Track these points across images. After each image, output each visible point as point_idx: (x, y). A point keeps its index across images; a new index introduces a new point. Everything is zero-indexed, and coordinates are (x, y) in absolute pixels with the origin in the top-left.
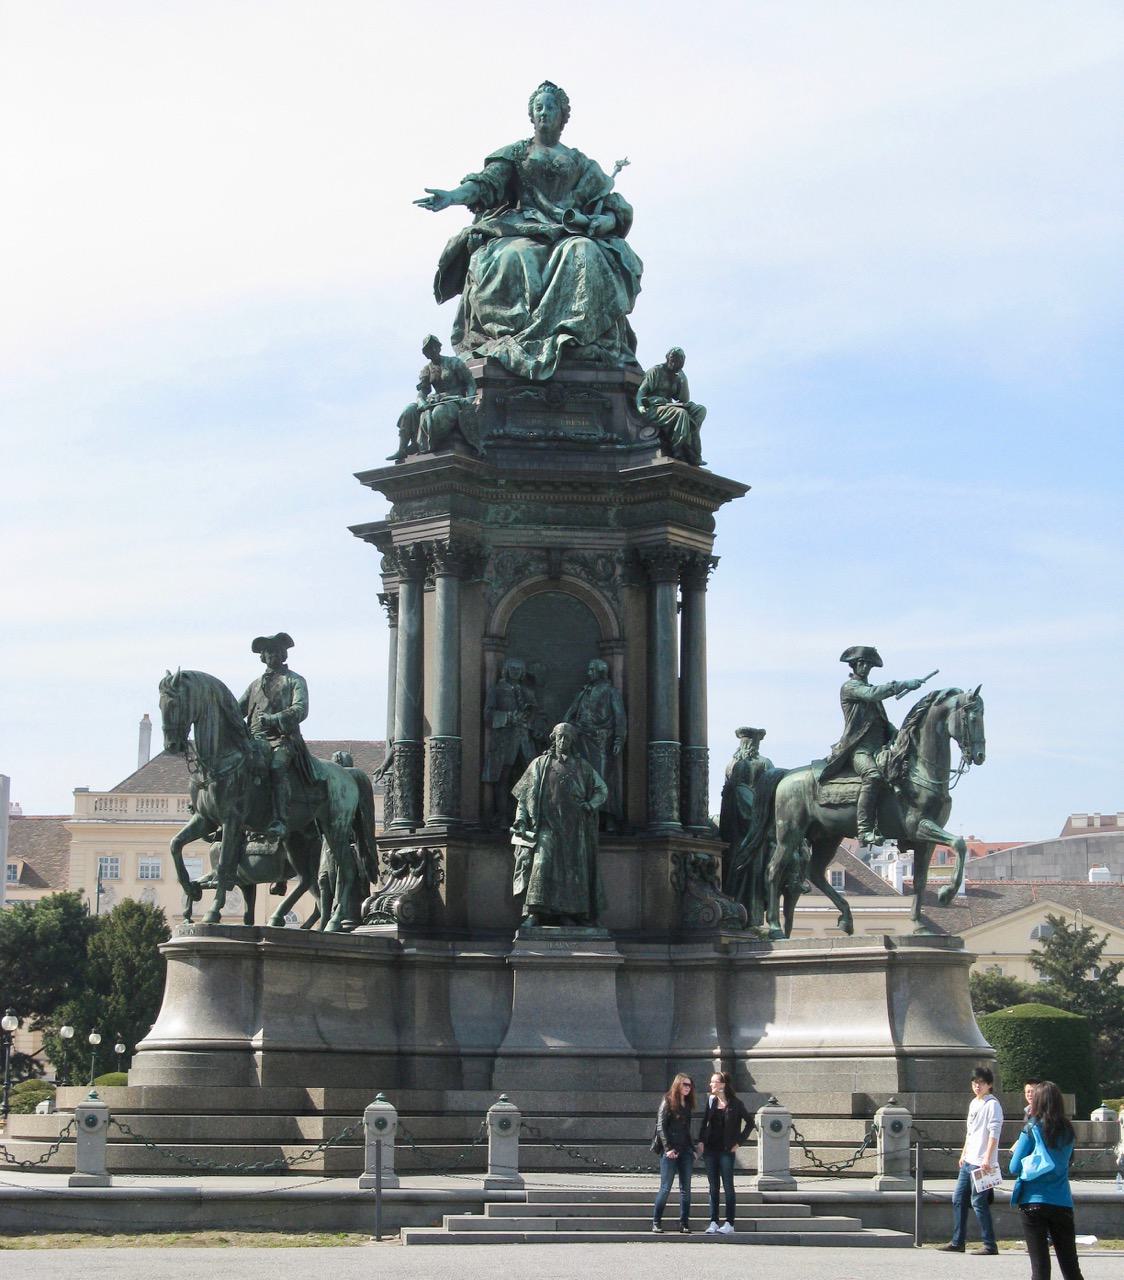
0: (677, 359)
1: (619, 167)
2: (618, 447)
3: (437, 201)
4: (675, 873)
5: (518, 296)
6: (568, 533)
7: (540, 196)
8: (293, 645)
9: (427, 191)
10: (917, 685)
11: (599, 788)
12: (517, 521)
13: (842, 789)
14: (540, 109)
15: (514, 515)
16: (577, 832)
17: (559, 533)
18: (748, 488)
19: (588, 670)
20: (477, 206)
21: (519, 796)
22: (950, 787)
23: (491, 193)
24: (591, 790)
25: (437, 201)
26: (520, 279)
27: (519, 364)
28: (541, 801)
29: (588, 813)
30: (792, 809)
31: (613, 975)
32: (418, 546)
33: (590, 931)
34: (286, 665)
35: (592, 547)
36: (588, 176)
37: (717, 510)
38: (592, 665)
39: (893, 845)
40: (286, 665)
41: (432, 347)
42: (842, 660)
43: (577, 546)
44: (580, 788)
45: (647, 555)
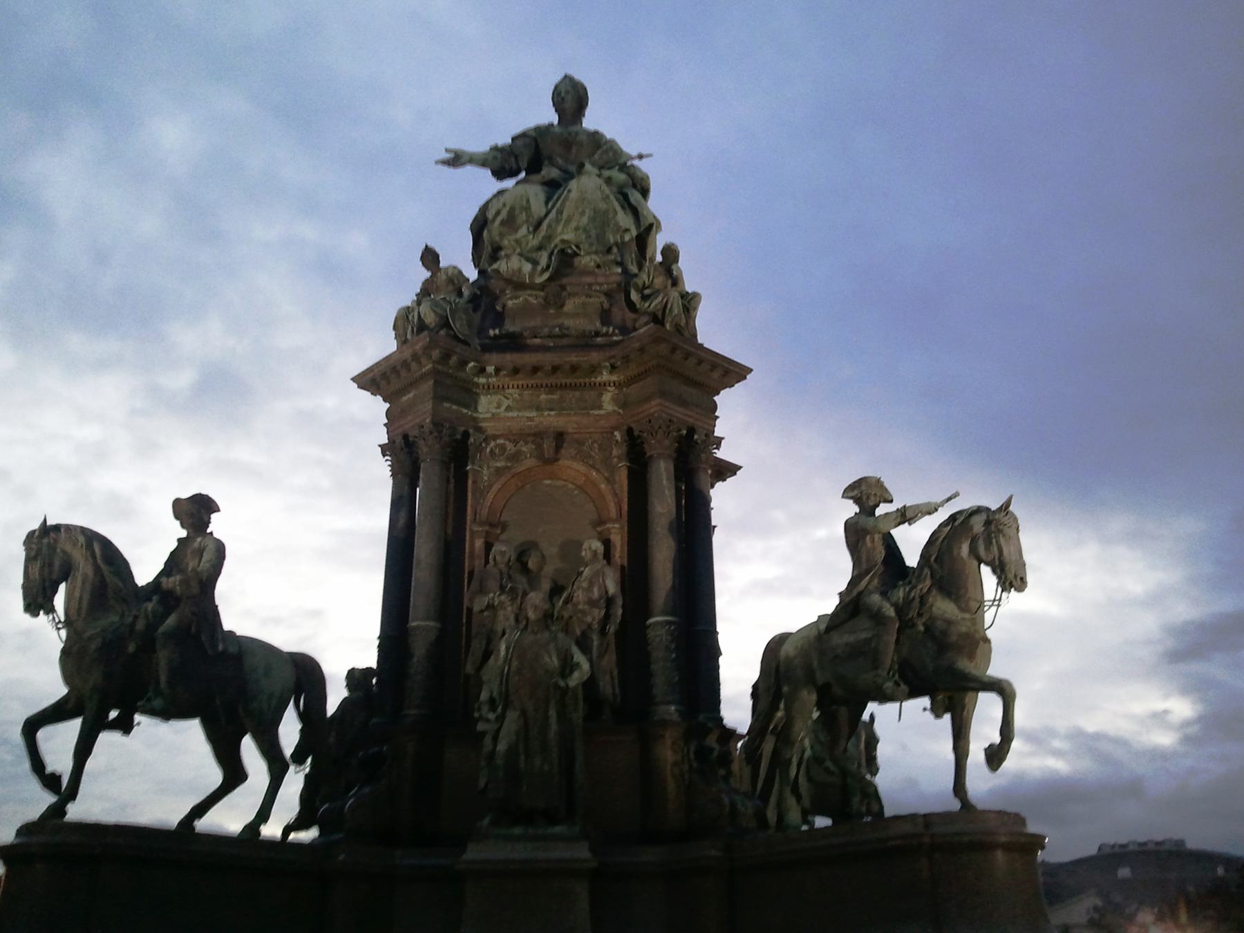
1: (640, 157)
3: (456, 160)
4: (675, 764)
8: (215, 509)
10: (931, 510)
11: (578, 665)
13: (851, 639)
15: (506, 403)
16: (547, 711)
18: (752, 370)
20: (499, 174)
22: (986, 626)
23: (513, 159)
24: (568, 666)
25: (456, 160)
26: (527, 208)
28: (507, 680)
29: (565, 691)
33: (558, 829)
34: (211, 533)
36: (605, 147)
37: (718, 394)
38: (585, 546)
39: (925, 709)
40: (211, 533)
41: (430, 257)
42: (843, 497)
44: (554, 661)
45: (640, 431)
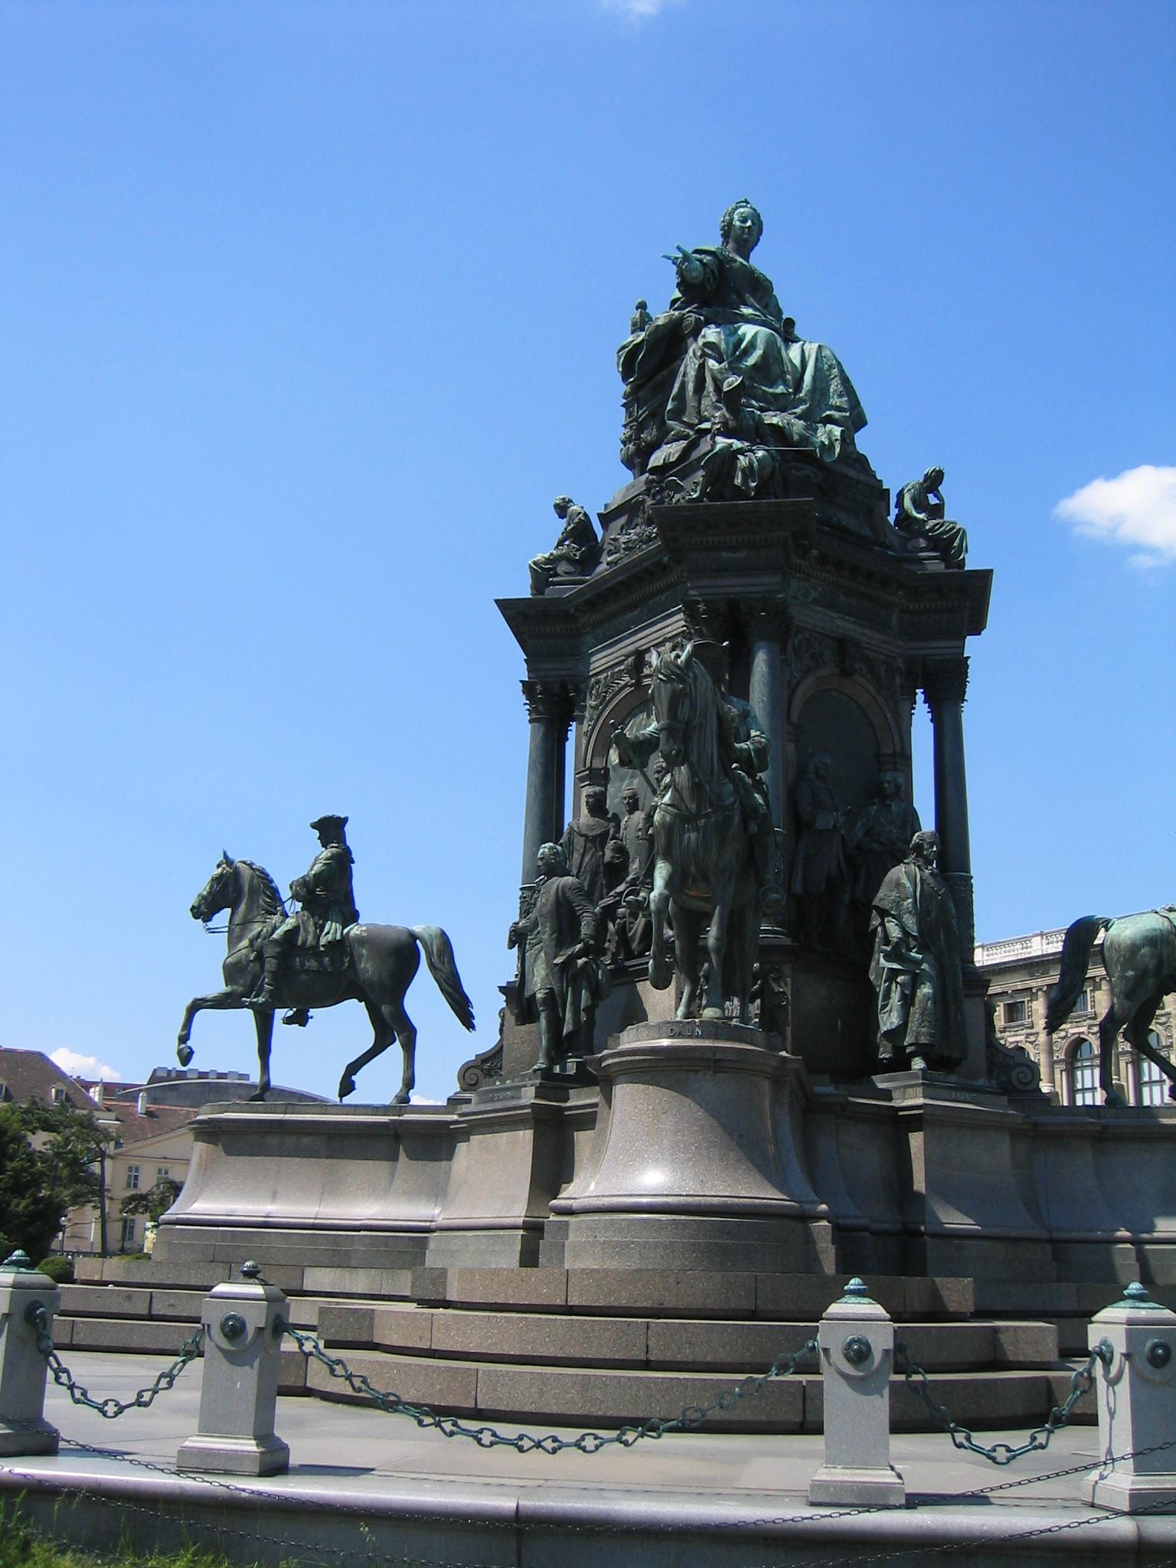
0: (934, 480)
2: (889, 552)
5: (778, 377)
6: (859, 630)
7: (752, 299)
9: (679, 248)
12: (815, 602)
14: (744, 221)
17: (850, 626)
19: (882, 783)
21: (892, 908)
27: (805, 440)
30: (1147, 959)
31: (1007, 1137)
32: (733, 605)
35: (876, 649)
43: (864, 645)
